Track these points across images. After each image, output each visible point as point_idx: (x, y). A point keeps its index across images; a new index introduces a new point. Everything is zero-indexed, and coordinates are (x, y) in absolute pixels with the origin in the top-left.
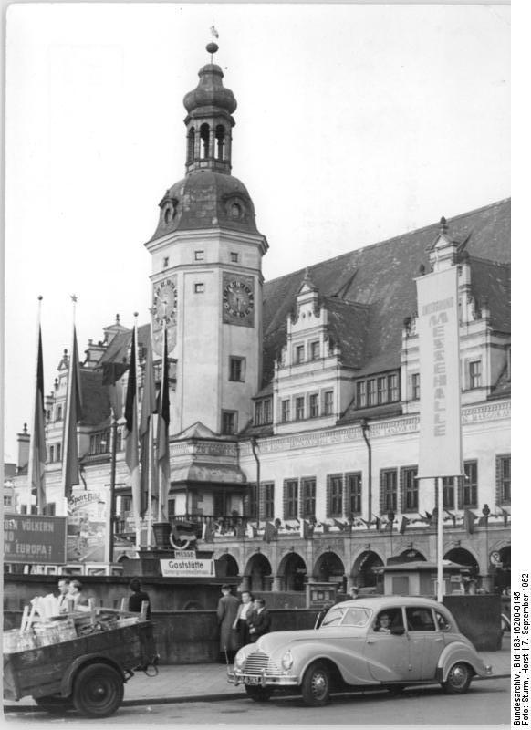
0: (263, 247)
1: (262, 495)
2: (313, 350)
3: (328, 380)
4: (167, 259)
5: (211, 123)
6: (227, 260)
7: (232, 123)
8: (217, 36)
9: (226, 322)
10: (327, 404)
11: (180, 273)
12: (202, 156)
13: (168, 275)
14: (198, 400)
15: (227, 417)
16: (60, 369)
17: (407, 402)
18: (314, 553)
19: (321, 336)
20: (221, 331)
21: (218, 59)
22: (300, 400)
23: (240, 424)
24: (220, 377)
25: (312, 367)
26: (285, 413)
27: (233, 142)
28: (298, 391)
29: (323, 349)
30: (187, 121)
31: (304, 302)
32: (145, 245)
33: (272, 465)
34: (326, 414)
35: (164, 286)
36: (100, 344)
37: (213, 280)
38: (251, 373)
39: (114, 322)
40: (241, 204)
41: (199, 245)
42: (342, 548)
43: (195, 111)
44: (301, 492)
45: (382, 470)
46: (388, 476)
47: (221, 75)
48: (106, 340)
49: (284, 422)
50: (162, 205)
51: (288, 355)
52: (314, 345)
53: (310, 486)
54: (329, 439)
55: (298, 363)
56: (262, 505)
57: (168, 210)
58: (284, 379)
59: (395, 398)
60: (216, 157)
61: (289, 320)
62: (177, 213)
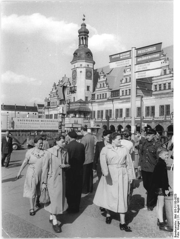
0: (94, 63)
1: (93, 114)
3: (107, 91)
4: (75, 66)
5: (83, 36)
7: (88, 36)
8: (85, 17)
9: (86, 79)
10: (106, 96)
11: (77, 69)
12: (82, 44)
13: (75, 69)
14: (81, 94)
15: (87, 98)
16: (53, 87)
17: (121, 96)
19: (105, 83)
20: (85, 81)
21: (85, 22)
22: (100, 95)
24: (85, 90)
25: (103, 88)
26: (98, 97)
27: (88, 41)
28: (100, 93)
29: (105, 85)
30: (79, 36)
31: (101, 76)
32: (71, 62)
33: (95, 108)
34: (106, 98)
35: (74, 72)
36: (62, 81)
37: (84, 70)
38: (91, 89)
39: (64, 76)
41: (81, 63)
43: (80, 34)
44: (100, 113)
45: (116, 109)
46: (117, 110)
47: (86, 26)
48: (63, 80)
50: (74, 54)
51: (98, 85)
52: (104, 84)
53: (102, 111)
54: (106, 103)
55: (101, 87)
56: (93, 115)
58: (97, 91)
60: (85, 44)
61: (99, 79)
62: (76, 56)
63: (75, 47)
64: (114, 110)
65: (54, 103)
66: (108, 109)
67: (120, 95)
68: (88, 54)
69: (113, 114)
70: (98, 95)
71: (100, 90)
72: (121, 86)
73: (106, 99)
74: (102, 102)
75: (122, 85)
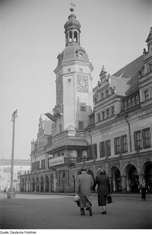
2: (107, 93)
3: (113, 102)
10: (113, 112)
15: (81, 124)
17: (143, 103)
18: (108, 168)
22: (103, 113)
23: (85, 125)
25: (106, 100)
26: (99, 118)
41: (69, 67)
42: (119, 164)
54: (114, 125)
57: (60, 59)
59: (138, 103)
63: (61, 47)
64: (132, 134)
65: (41, 143)
66: (120, 135)
67: (141, 101)
68: (79, 53)
69: (131, 143)
70: (99, 115)
71: (102, 104)
72: (141, 83)
73: (113, 118)
74: (106, 124)
75: (143, 79)
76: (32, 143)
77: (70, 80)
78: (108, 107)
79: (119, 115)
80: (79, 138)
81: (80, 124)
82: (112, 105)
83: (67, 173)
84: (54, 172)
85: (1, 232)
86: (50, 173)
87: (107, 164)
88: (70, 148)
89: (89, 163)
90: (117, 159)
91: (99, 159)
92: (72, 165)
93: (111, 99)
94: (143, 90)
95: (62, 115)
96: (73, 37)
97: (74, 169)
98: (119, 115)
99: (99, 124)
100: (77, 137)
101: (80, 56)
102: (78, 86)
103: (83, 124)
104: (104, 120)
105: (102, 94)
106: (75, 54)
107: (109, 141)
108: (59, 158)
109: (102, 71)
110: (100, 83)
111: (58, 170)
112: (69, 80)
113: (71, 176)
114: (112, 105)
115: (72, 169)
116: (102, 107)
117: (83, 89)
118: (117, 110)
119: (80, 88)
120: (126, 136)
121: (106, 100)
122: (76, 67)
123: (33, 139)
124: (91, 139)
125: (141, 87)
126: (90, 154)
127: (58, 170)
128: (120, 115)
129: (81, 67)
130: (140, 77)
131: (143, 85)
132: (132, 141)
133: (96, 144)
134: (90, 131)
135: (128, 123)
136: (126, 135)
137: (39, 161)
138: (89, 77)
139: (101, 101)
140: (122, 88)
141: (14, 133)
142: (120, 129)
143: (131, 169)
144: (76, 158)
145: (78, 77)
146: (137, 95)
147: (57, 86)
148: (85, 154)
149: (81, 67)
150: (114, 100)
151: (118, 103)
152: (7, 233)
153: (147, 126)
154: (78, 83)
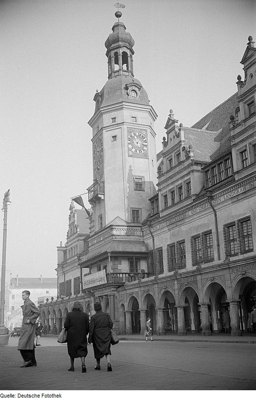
2: (178, 158)
3: (188, 174)
6: (130, 120)
10: (189, 191)
15: (135, 213)
17: (238, 172)
18: (179, 289)
22: (173, 192)
23: (144, 216)
25: (177, 169)
26: (166, 203)
40: (136, 89)
41: (113, 114)
42: (196, 282)
44: (177, 249)
49: (166, 208)
54: (190, 213)
59: (230, 174)
66: (200, 232)
67: (235, 170)
68: (130, 89)
70: (166, 196)
71: (170, 178)
72: (234, 137)
73: (189, 201)
75: (237, 130)
76: (59, 249)
77: (116, 136)
78: (180, 182)
79: (200, 196)
80: (132, 238)
81: (133, 214)
82: (186, 178)
83: (111, 299)
84: (92, 299)
85: (2, 396)
86: (87, 300)
87: (176, 282)
88: (117, 256)
89: (147, 282)
90: (194, 274)
91: (166, 273)
92: (120, 286)
93: (185, 169)
94: (238, 150)
95: (103, 198)
96: (121, 61)
97: (123, 293)
98: (200, 196)
99: (165, 213)
100: (129, 237)
101: (133, 94)
102: (130, 146)
103: (140, 213)
104: (174, 204)
105: (170, 160)
106: (124, 92)
107: (183, 242)
108: (97, 273)
109: (169, 119)
110: (166, 141)
111: (97, 294)
112: (115, 137)
113: (120, 305)
114: (186, 178)
115: (121, 293)
116: (170, 182)
117: (138, 151)
118: (196, 188)
119: (133, 150)
120: (210, 232)
121: (177, 169)
122: (125, 115)
123: (61, 242)
124: (153, 240)
125: (235, 145)
126: (151, 266)
127: (97, 294)
128: (200, 195)
129: (135, 114)
130: (232, 126)
131: (237, 140)
132: (220, 242)
133: (161, 247)
134: (150, 226)
135: (213, 209)
136: (211, 230)
137: (70, 281)
138: (149, 130)
139: (168, 172)
140: (204, 149)
141: (5, 230)
142: (201, 221)
143: (218, 292)
144: (127, 273)
145: (130, 131)
146: (229, 159)
147: (95, 147)
148: (143, 266)
149: (135, 114)
150: (190, 170)
151: (196, 174)
152: (13, 396)
153: (245, 214)
154: (129, 142)
